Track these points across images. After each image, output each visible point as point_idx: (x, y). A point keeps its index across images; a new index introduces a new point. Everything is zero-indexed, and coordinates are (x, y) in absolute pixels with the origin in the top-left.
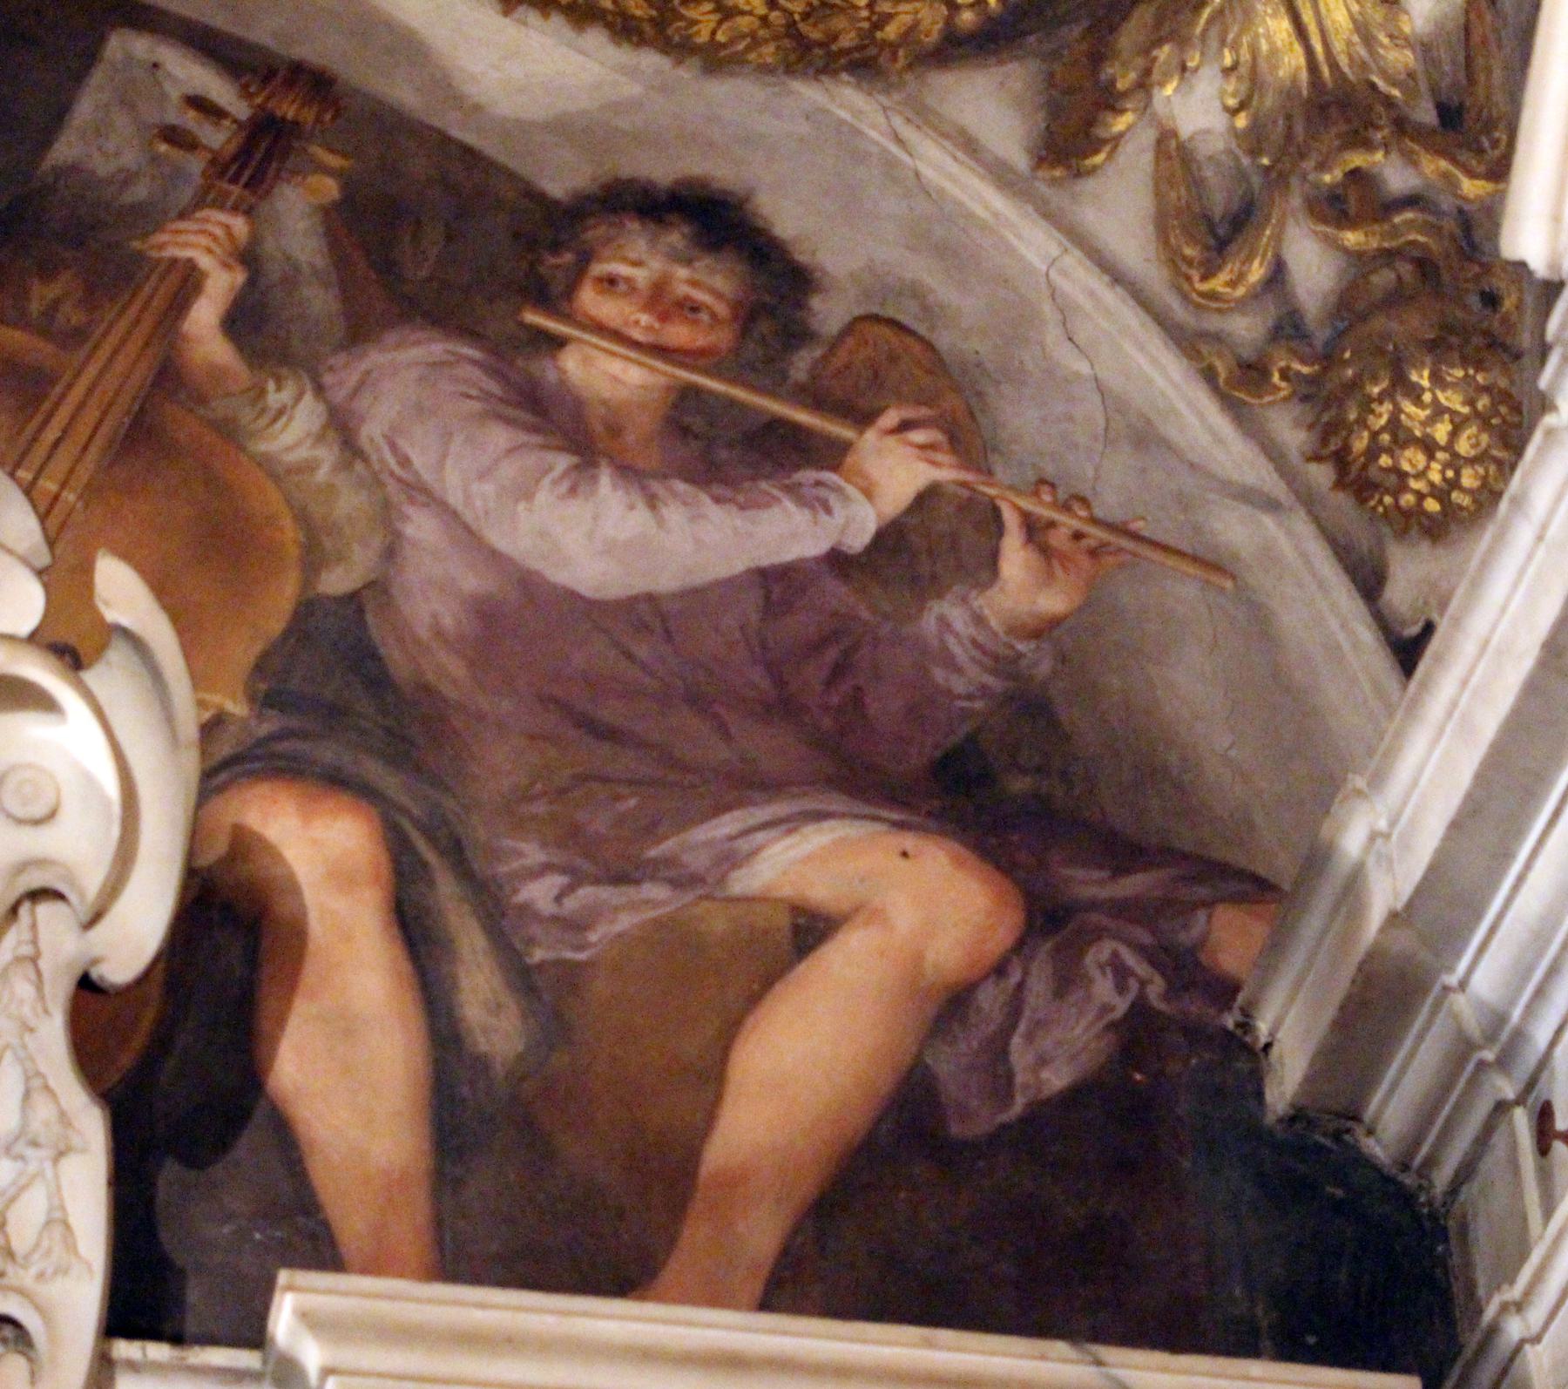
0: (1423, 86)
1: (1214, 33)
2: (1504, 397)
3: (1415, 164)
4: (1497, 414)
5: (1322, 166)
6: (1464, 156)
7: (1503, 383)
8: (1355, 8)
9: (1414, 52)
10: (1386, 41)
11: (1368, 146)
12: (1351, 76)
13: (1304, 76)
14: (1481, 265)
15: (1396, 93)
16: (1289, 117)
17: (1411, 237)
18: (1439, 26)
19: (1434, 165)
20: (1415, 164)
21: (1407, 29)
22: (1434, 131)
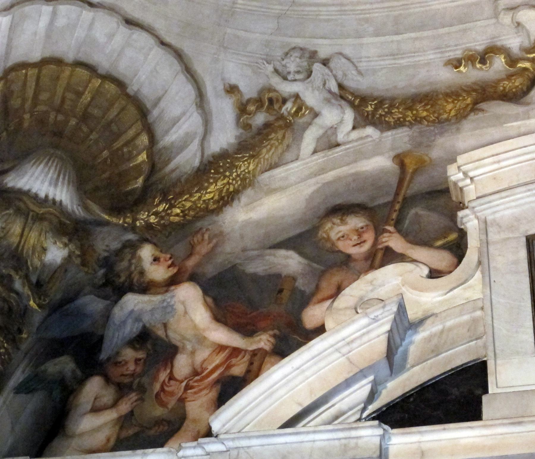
0: (38, 272)
1: (5, 217)
2: (9, 354)
3: (24, 287)
4: (4, 356)
5: (5, 267)
6: (36, 296)
7: (11, 351)
8: (36, 243)
9: (41, 263)
10: (37, 256)
11: (17, 274)
12: (24, 255)
13: (15, 245)
14: (23, 321)
15: (31, 268)
16: (6, 250)
17: (12, 301)
18: (51, 264)
19: (26, 291)
20: (24, 287)
21: (43, 258)
22: (32, 284)
